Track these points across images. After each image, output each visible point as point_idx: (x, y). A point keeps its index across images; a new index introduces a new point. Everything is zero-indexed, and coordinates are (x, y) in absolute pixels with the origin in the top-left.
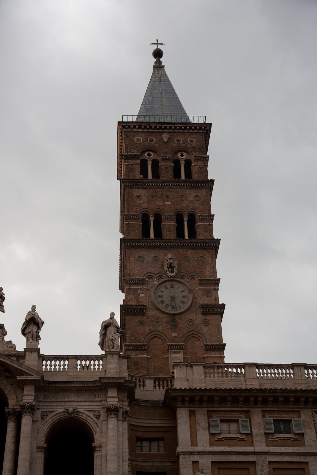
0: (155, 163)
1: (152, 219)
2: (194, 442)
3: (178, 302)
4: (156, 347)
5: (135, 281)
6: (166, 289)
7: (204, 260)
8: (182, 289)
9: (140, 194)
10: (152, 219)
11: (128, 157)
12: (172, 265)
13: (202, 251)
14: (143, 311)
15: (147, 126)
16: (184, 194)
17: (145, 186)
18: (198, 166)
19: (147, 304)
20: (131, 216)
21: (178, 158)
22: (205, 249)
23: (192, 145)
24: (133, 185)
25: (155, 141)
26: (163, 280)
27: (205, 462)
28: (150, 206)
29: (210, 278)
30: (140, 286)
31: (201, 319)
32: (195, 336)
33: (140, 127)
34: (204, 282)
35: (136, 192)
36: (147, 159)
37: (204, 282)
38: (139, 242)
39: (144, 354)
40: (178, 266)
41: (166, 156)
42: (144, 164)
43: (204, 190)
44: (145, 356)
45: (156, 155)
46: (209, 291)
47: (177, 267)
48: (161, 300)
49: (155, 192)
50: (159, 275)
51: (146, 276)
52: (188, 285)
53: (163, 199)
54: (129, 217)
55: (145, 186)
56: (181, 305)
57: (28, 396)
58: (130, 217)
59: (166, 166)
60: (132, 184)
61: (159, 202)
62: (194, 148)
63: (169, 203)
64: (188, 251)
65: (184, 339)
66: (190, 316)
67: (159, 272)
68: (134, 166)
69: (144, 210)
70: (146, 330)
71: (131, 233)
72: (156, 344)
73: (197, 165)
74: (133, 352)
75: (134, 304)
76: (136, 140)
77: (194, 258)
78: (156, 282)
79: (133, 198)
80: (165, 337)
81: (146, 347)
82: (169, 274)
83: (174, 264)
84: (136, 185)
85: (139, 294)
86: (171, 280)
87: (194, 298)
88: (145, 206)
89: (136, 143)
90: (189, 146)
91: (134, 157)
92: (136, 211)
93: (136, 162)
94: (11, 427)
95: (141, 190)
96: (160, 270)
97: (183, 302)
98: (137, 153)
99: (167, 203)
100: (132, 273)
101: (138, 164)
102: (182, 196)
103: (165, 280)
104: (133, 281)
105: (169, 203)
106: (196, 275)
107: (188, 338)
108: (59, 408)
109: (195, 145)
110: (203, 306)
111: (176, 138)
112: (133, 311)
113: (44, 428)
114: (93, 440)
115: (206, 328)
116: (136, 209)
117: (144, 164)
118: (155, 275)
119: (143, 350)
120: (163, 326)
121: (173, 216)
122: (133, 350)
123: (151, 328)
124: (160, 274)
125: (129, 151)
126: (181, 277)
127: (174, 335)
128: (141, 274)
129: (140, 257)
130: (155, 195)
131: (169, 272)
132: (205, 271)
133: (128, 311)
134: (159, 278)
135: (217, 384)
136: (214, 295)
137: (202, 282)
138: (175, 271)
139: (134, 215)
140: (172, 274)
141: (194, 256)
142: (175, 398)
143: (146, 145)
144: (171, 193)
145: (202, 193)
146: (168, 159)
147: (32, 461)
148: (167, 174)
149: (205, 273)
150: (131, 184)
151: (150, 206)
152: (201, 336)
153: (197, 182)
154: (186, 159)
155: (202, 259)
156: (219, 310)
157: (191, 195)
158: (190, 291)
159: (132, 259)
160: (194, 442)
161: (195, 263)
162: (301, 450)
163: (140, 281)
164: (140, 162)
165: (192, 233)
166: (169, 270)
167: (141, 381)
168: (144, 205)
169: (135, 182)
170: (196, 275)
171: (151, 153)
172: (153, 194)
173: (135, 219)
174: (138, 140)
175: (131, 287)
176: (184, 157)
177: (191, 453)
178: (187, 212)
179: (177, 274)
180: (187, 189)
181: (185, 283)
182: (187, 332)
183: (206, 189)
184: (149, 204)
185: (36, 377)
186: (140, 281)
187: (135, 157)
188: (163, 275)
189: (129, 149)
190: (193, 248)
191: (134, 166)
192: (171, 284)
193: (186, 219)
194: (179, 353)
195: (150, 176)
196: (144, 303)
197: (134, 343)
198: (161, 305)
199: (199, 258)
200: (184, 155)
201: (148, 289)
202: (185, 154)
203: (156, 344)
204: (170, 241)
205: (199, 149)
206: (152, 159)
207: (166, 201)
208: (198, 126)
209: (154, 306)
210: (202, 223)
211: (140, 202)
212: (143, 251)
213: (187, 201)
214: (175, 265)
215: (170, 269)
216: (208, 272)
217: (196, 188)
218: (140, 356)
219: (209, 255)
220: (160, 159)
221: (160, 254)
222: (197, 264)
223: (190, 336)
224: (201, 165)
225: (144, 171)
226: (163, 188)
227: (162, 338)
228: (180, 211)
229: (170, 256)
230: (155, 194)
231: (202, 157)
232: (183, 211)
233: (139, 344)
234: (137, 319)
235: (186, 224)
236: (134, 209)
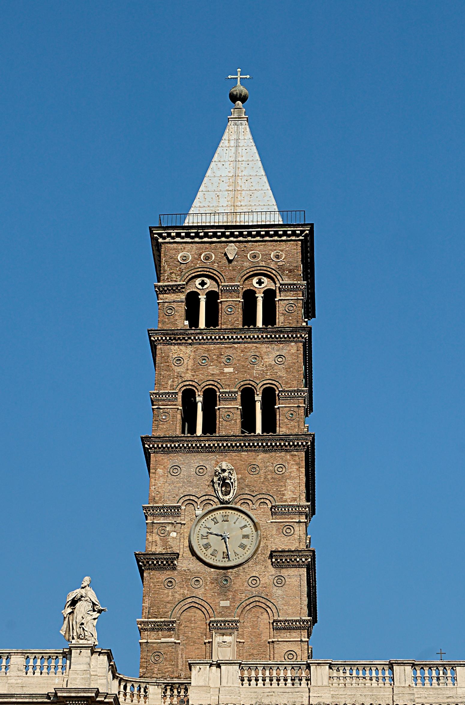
0: (212, 297)
1: (199, 399)
3: (233, 547)
4: (193, 625)
5: (162, 511)
6: (215, 523)
7: (284, 471)
8: (243, 520)
9: (181, 355)
11: (163, 289)
12: (228, 481)
13: (283, 454)
14: (172, 562)
15: (201, 232)
16: (257, 354)
17: (190, 341)
18: (285, 302)
19: (182, 550)
20: (163, 394)
21: (251, 288)
22: (286, 451)
23: (279, 264)
24: (170, 338)
25: (213, 259)
26: (211, 508)
28: (197, 375)
29: (292, 504)
30: (171, 518)
31: (272, 575)
32: (260, 604)
34: (281, 509)
35: (175, 351)
36: (198, 291)
37: (281, 509)
38: (173, 442)
39: (170, 636)
40: (239, 483)
41: (232, 286)
42: (192, 300)
43: (293, 344)
44: (172, 640)
45: (214, 283)
46: (290, 527)
47: (236, 484)
48: (205, 543)
49: (208, 351)
50: (204, 498)
51: (182, 501)
52: (253, 517)
53: (220, 363)
54: (159, 396)
55: (190, 341)
56: (239, 551)
58: (161, 396)
60: (168, 338)
62: (281, 268)
63: (231, 370)
64: (258, 456)
65: (239, 611)
66: (254, 570)
67: (205, 494)
68: (174, 305)
69: (188, 383)
70: (177, 595)
71: (162, 424)
72: (193, 619)
73: (285, 300)
74: (153, 633)
75: (159, 550)
76: (180, 257)
77: (267, 467)
78: (199, 512)
79: (168, 362)
80: (208, 607)
81: (174, 625)
82: (221, 496)
83: (231, 479)
84: (175, 339)
85: (169, 533)
86: (225, 506)
88: (188, 376)
89: (181, 263)
90: (272, 266)
91: (175, 289)
92: (171, 386)
93: (178, 297)
95: (182, 348)
96: (207, 490)
97: (243, 546)
98: (180, 281)
99: (226, 370)
100: (159, 495)
101: (182, 302)
102: (255, 357)
103: (215, 507)
104: (160, 510)
105: (231, 370)
106: (270, 498)
107: (248, 608)
109: (284, 263)
111: (250, 253)
112: (155, 562)
115: (280, 592)
116: (173, 381)
118: (199, 498)
119: (169, 630)
120: (207, 588)
121: (236, 392)
122: (153, 630)
123: (186, 592)
124: (207, 497)
125: (167, 279)
126: (242, 501)
127: (224, 603)
128: (174, 497)
130: (208, 356)
131: (222, 493)
132: (285, 490)
133: (148, 562)
135: (260, 697)
136: (297, 532)
137: (278, 509)
138: (232, 491)
139: (169, 393)
140: (226, 498)
141: (268, 464)
143: (198, 265)
144: (234, 351)
145: (290, 350)
146: (234, 291)
149: (284, 495)
150: (166, 338)
151: (197, 375)
152: (270, 605)
153: (281, 332)
154: (266, 289)
155: (280, 470)
156: (304, 560)
157: (270, 353)
159: (160, 471)
161: (269, 477)
163: (171, 510)
164: (186, 299)
165: (270, 424)
166: (221, 490)
167: (142, 690)
168: (187, 375)
169: (172, 334)
170: (270, 498)
171: (206, 280)
172: (204, 355)
173: (169, 401)
175: (155, 522)
176: (263, 285)
178: (260, 385)
179: (235, 498)
180: (263, 343)
181: (249, 513)
182: (247, 598)
183: (296, 342)
184: (195, 372)
186: (171, 510)
187: (177, 288)
188: (212, 498)
189: (168, 275)
190: (267, 449)
191: (174, 305)
192: (224, 514)
193: (258, 398)
194: (230, 634)
195: (202, 324)
197: (154, 617)
198: (205, 551)
199: (276, 468)
200: (263, 283)
201: (184, 524)
202: (265, 279)
203: (193, 619)
204: (226, 438)
205: (290, 271)
206: (208, 291)
207: (226, 366)
208: (289, 229)
209: (193, 553)
210: (285, 404)
211: (181, 369)
212: (181, 456)
213: (263, 365)
214: (232, 481)
215: (223, 489)
216: (290, 493)
218: (163, 640)
219: (293, 463)
222: (272, 478)
223: (251, 606)
224: (292, 300)
225: (192, 316)
226: (223, 343)
227: (203, 609)
228: (249, 384)
230: (206, 355)
231: (294, 284)
232: (253, 384)
233: (163, 620)
234: (163, 576)
235: (258, 405)
236: (170, 382)
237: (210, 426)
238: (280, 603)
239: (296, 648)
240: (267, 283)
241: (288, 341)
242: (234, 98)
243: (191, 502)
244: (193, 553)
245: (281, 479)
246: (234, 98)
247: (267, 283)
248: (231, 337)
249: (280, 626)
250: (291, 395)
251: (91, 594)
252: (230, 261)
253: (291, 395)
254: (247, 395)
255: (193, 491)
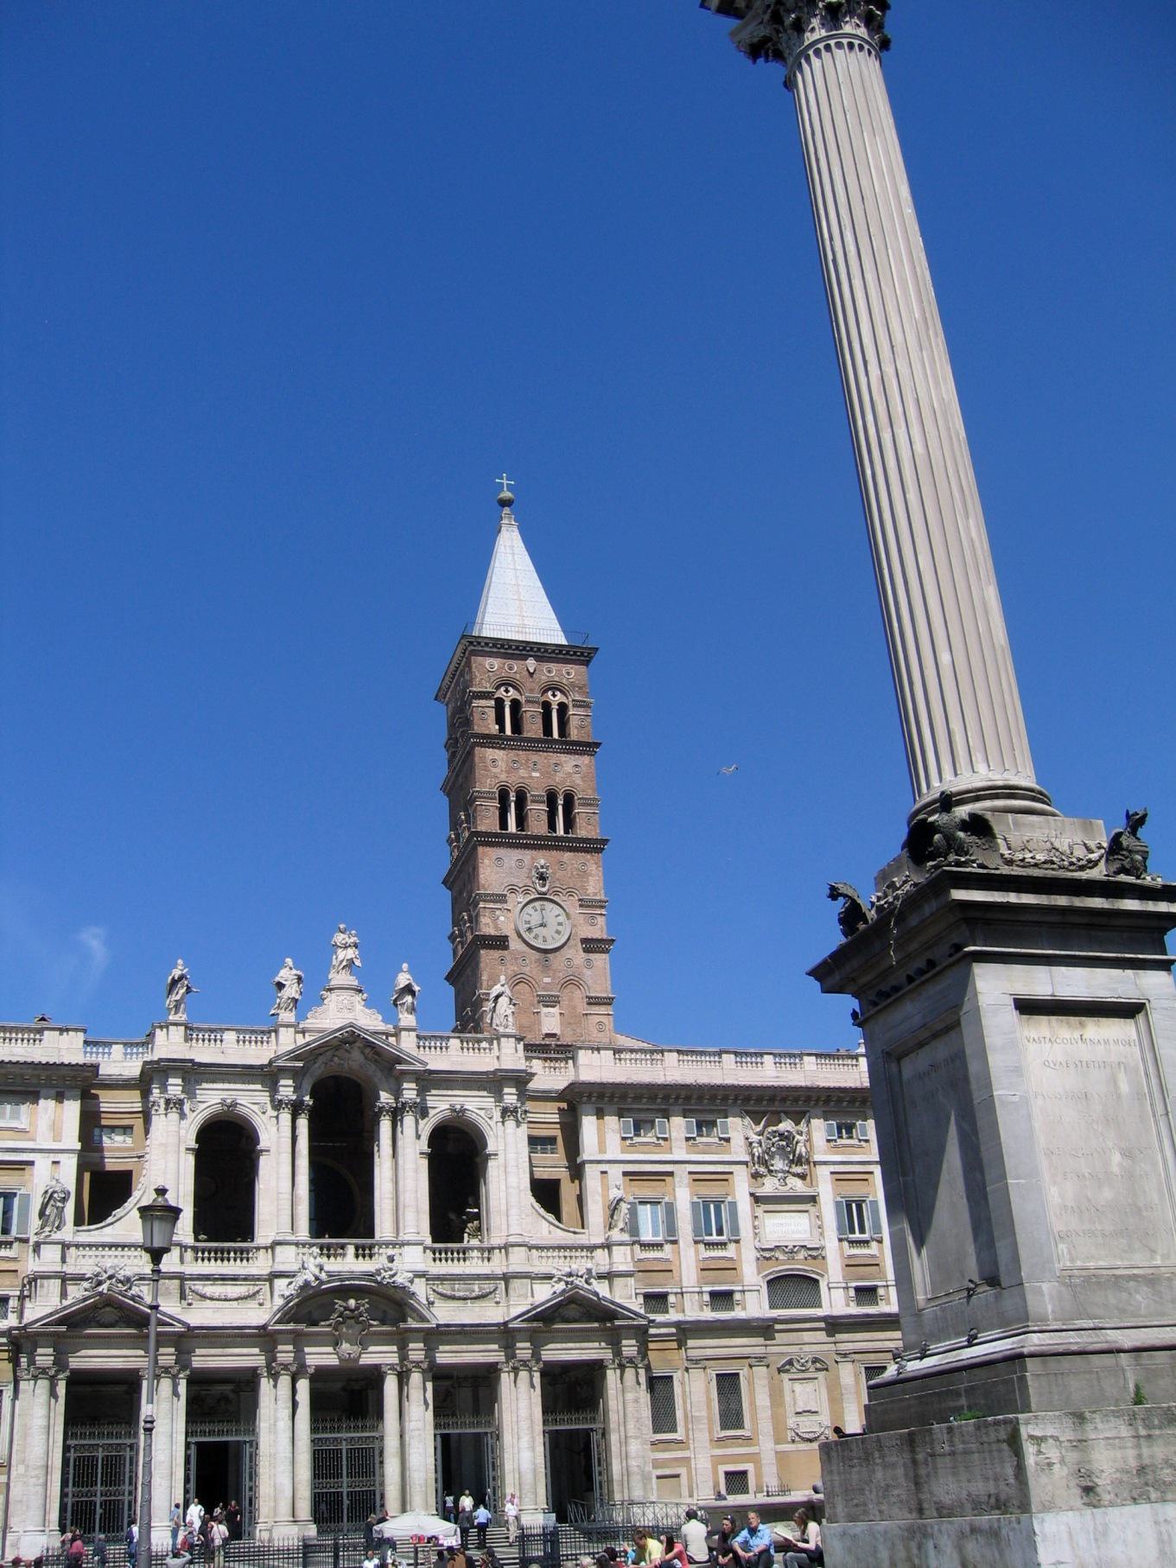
0: (516, 705)
1: (513, 798)
2: (602, 1147)
10: (513, 798)
27: (615, 1172)
33: (494, 646)
35: (490, 753)
42: (500, 703)
57: (410, 1092)
59: (532, 714)
61: (523, 773)
62: (573, 685)
66: (568, 952)
86: (542, 898)
87: (574, 926)
88: (503, 777)
94: (385, 1125)
97: (558, 932)
102: (556, 765)
108: (441, 1104)
110: (584, 941)
113: (426, 1127)
114: (485, 1145)
115: (588, 972)
117: (500, 703)
127: (547, 980)
129: (499, 859)
134: (526, 892)
142: (581, 1095)
147: (416, 1171)
148: (533, 728)
157: (569, 762)
158: (568, 915)
160: (602, 1147)
162: (726, 1158)
174: (492, 666)
177: (599, 1162)
185: (419, 1067)
190: (571, 849)
193: (561, 802)
196: (505, 932)
209: (520, 936)
217: (576, 753)
220: (522, 699)
221: (527, 855)
225: (500, 720)
229: (542, 862)
234: (496, 954)
237: (521, 822)
238: (589, 982)
239: (604, 1019)
240: (559, 697)
241: (582, 753)
242: (504, 503)
243: (513, 891)
244: (520, 936)
245: (584, 875)
246: (504, 503)
247: (559, 697)
248: (533, 745)
249: (594, 1001)
250: (587, 803)
251: (508, 992)
252: (531, 675)
253: (587, 803)
254: (551, 798)
255: (515, 881)
